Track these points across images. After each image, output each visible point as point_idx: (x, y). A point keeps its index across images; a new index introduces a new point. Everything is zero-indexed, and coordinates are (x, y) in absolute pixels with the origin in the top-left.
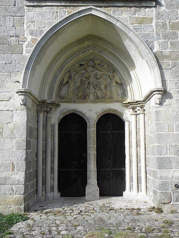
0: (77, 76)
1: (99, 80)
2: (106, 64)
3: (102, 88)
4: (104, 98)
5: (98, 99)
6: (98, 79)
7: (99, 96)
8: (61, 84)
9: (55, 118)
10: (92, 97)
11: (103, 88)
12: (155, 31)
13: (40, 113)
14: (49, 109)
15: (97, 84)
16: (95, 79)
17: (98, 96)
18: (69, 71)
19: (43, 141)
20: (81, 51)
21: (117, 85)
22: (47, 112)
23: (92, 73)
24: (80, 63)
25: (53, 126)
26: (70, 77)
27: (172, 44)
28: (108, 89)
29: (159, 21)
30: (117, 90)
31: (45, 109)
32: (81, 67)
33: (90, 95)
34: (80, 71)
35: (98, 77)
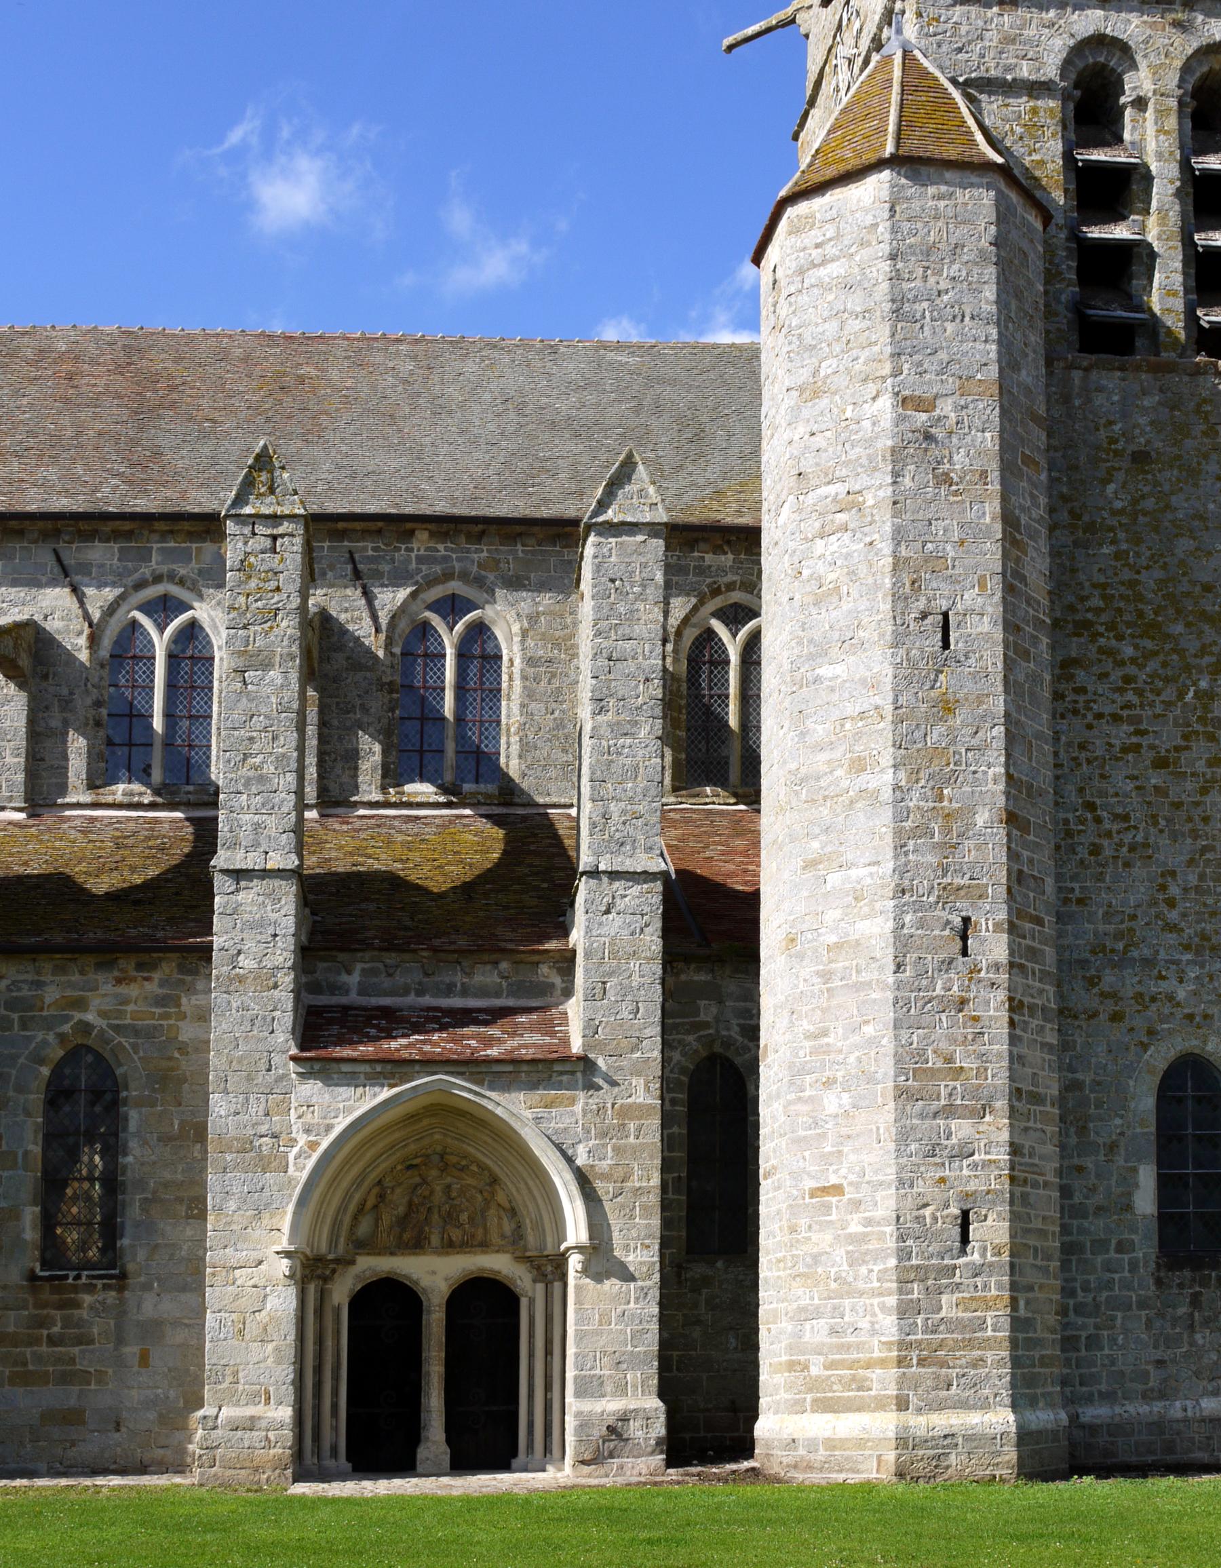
5: (449, 1247)
7: (454, 1239)
9: (341, 1292)
10: (435, 1240)
12: (581, 1122)
13: (309, 1283)
14: (328, 1272)
19: (315, 1343)
21: (502, 1213)
22: (325, 1279)
25: (338, 1309)
27: (616, 1149)
29: (590, 1101)
30: (500, 1226)
31: (319, 1272)
35: (454, 1194)
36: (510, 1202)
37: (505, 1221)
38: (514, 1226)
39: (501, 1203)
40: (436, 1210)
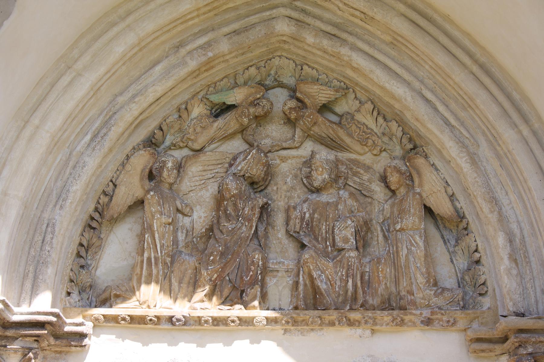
0: (194, 170)
1: (324, 198)
2: (369, 106)
3: (340, 244)
4: (355, 298)
6: (318, 190)
7: (323, 286)
8: (97, 216)
11: (346, 240)
15: (312, 218)
16: (299, 193)
17: (316, 290)
18: (151, 143)
20: (226, 30)
21: (433, 230)
23: (283, 159)
24: (216, 99)
26: (151, 176)
28: (378, 245)
32: (220, 122)
33: (271, 283)
34: (212, 141)
36: (452, 197)
37: (440, 251)
38: (462, 263)
39: (432, 203)
40: (279, 219)
